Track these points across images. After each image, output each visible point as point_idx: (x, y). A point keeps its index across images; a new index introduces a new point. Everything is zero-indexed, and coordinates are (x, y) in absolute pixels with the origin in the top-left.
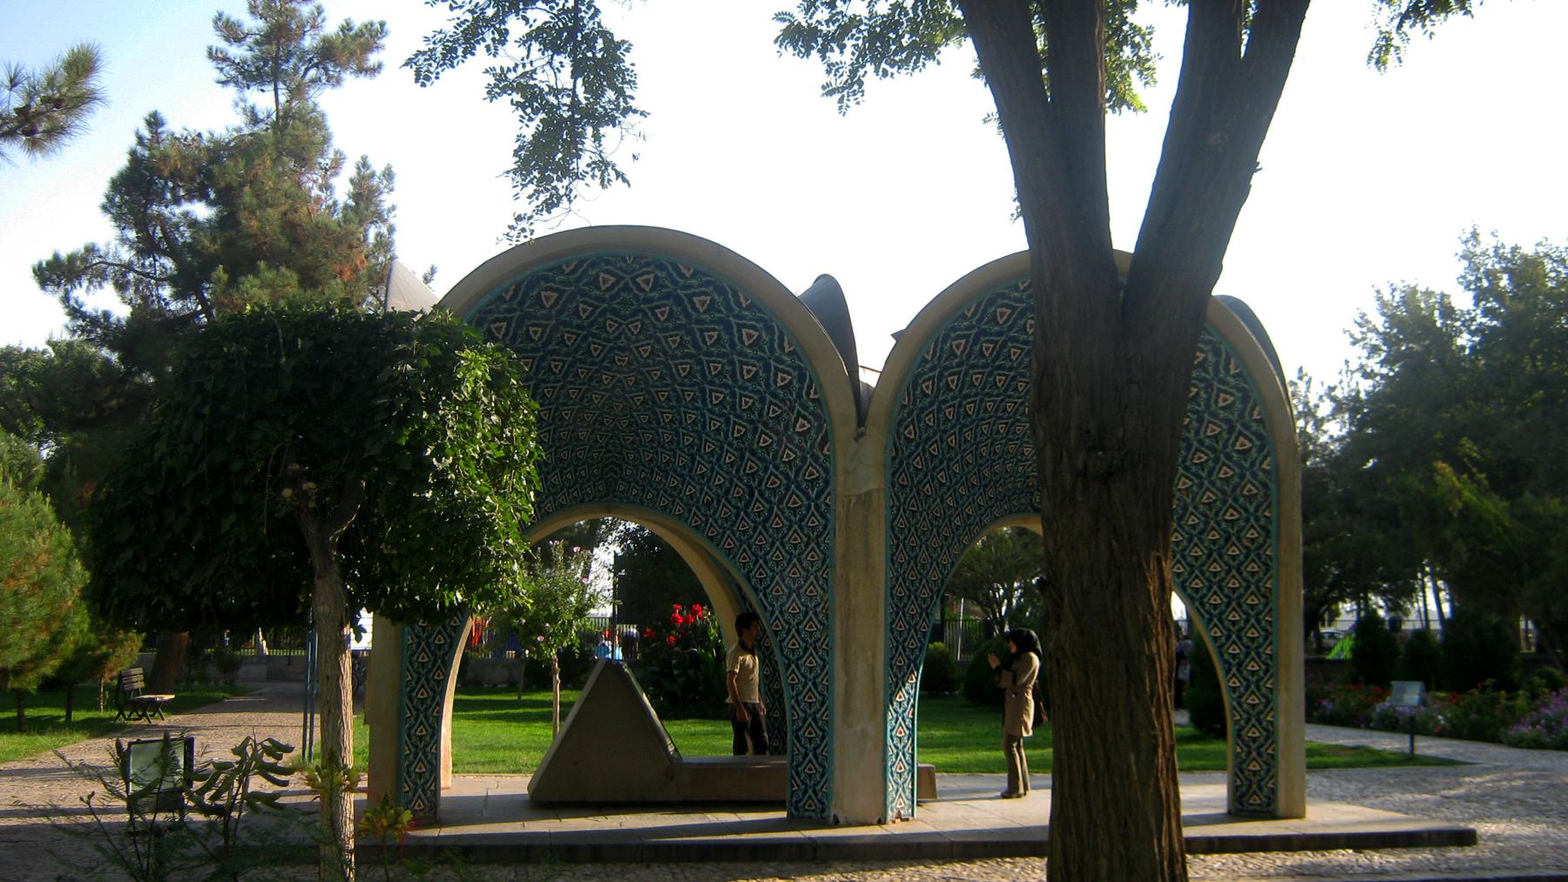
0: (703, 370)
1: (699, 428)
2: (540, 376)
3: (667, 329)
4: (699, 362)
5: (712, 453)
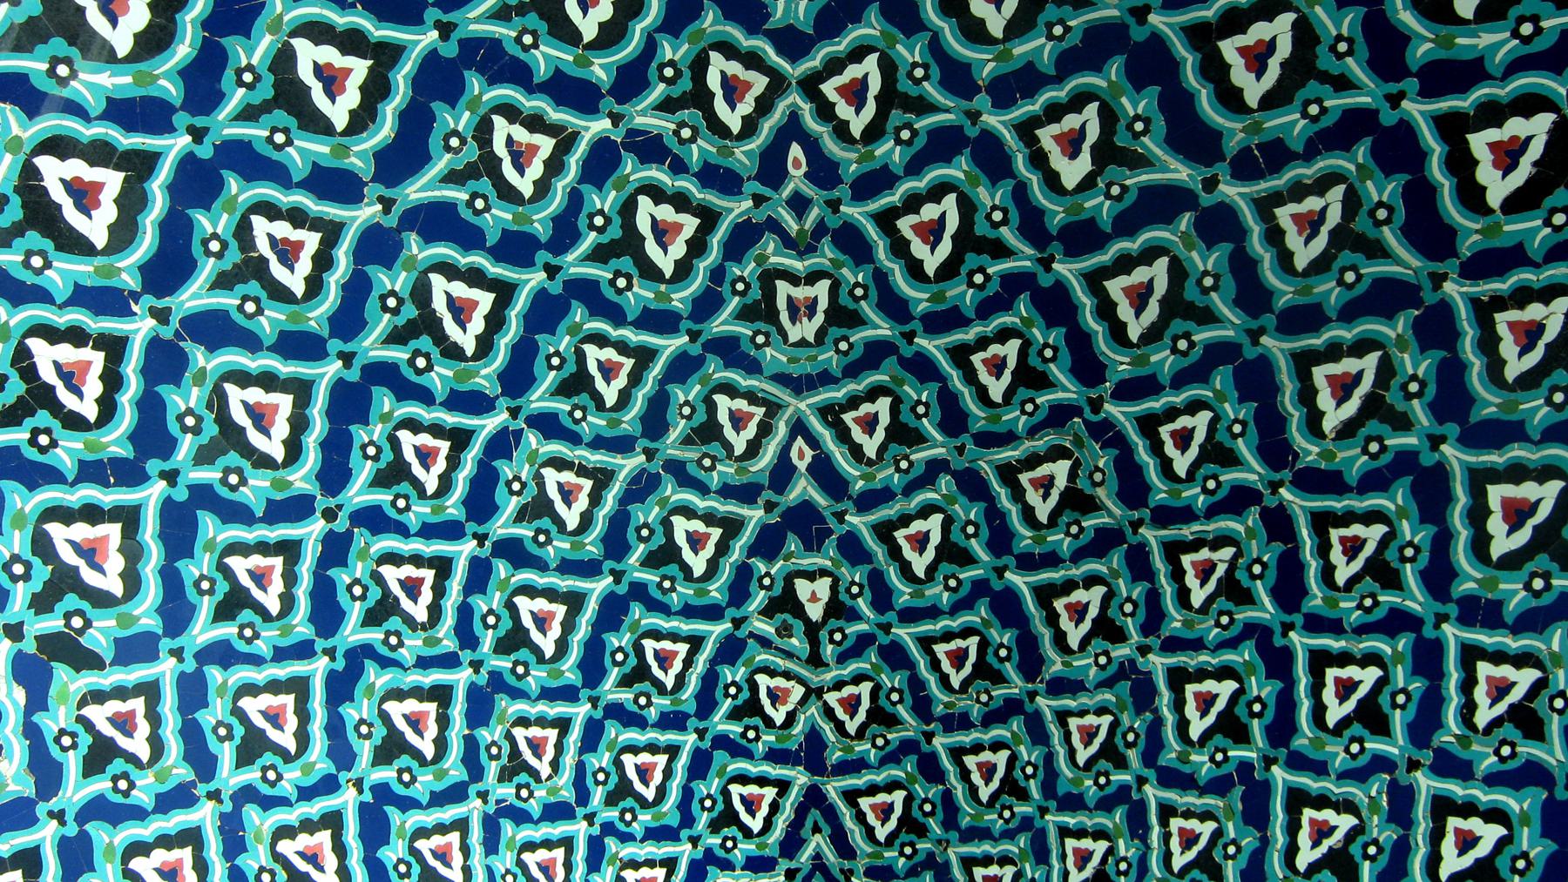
0: (1243, 266)
1: (1266, 610)
2: (371, 346)
3: (1023, 82)
4: (1219, 225)
5: (1371, 716)
